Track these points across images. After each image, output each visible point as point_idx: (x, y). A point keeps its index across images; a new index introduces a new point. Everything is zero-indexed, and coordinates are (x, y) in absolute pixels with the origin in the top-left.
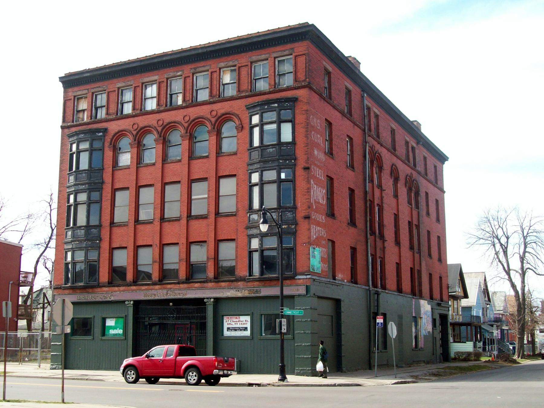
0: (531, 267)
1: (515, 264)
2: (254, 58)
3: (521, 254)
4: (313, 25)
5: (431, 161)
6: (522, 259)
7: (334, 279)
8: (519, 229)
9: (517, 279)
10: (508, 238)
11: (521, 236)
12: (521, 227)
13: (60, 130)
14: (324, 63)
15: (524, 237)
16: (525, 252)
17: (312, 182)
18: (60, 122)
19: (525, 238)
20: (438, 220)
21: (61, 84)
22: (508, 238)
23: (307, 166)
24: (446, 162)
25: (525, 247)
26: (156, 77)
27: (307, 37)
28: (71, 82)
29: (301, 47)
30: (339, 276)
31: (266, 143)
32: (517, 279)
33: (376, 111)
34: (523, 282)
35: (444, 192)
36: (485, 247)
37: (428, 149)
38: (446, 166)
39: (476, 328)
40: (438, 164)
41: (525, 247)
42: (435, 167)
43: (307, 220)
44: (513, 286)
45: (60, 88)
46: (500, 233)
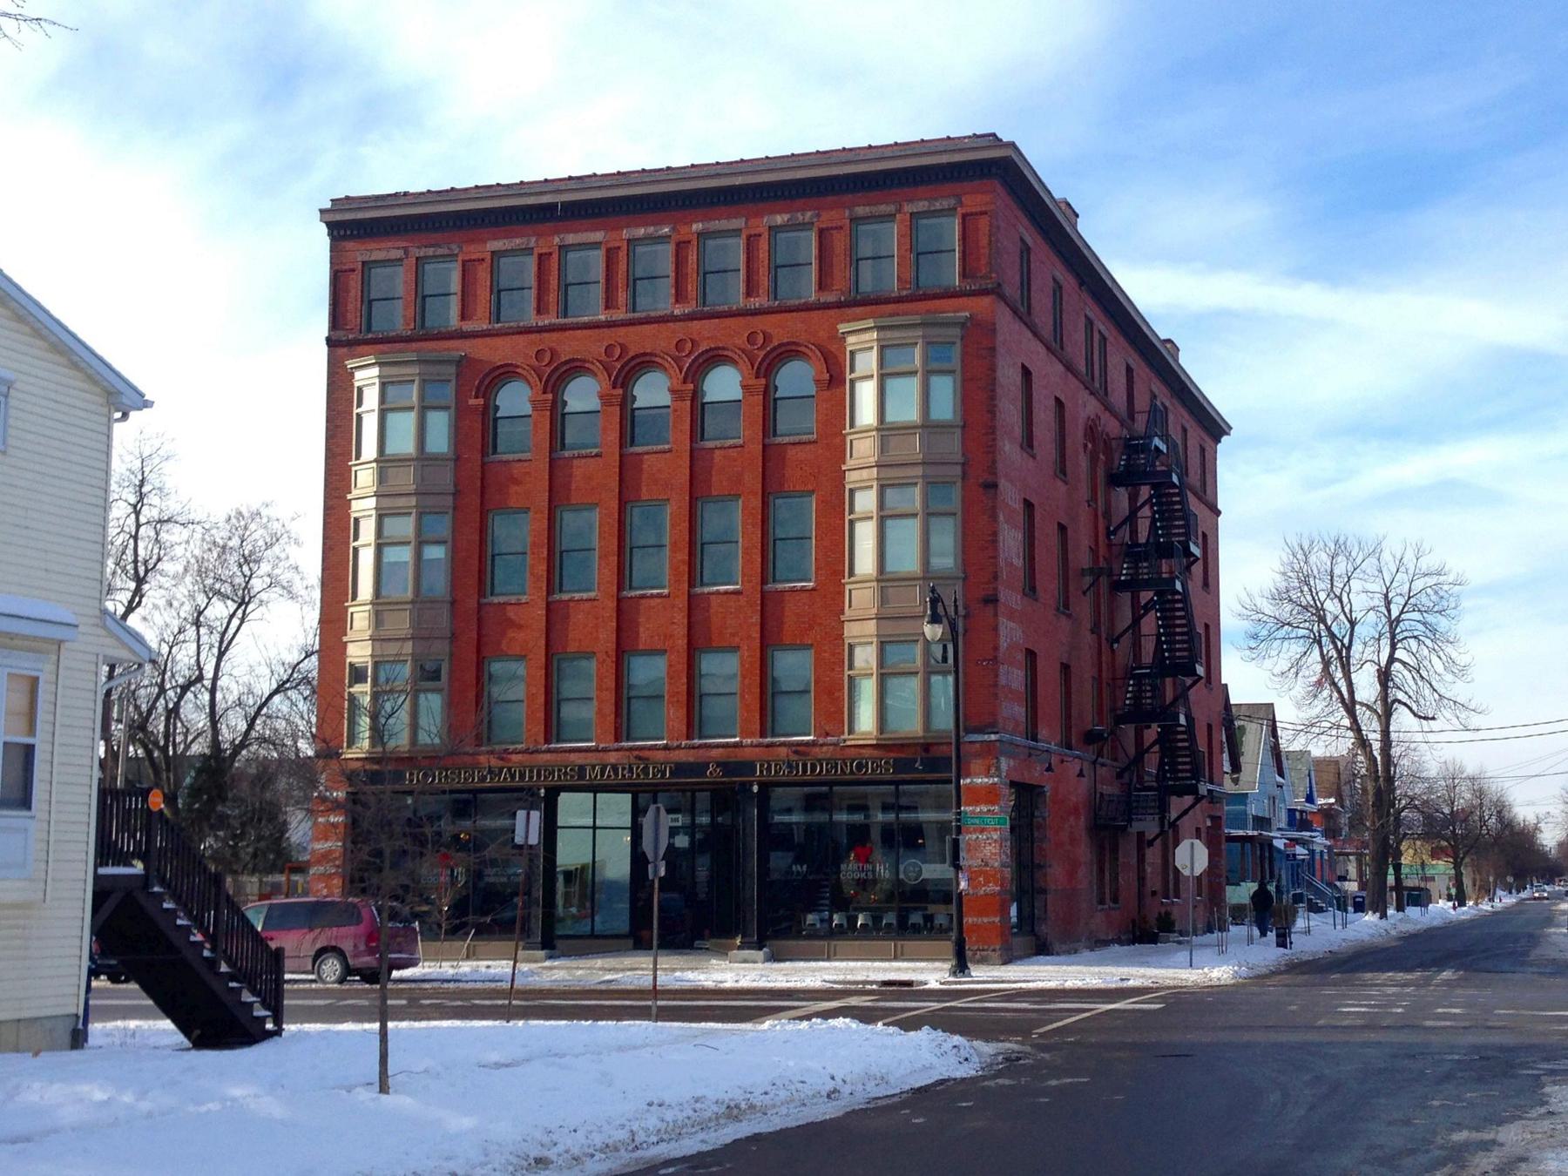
0: (1404, 698)
1: (1366, 686)
2: (861, 211)
3: (1383, 664)
4: (1012, 145)
5: (1195, 435)
6: (1385, 676)
7: (1034, 738)
8: (1378, 601)
9: (1371, 729)
10: (1353, 623)
11: (1384, 620)
12: (1386, 596)
13: (325, 348)
14: (1022, 230)
15: (1391, 623)
16: (1392, 659)
17: (1001, 518)
18: (324, 330)
19: (1393, 623)
20: (1206, 584)
21: (323, 229)
22: (1353, 623)
23: (990, 479)
24: (1224, 439)
25: (1393, 647)
26: (598, 236)
27: (994, 170)
28: (357, 227)
29: (977, 198)
30: (1043, 732)
31: (891, 417)
32: (1371, 729)
33: (1102, 328)
34: (1386, 733)
35: (1218, 513)
36: (1296, 648)
37: (1191, 412)
38: (1224, 446)
39: (1262, 846)
40: (1209, 441)
41: (1393, 647)
42: (1203, 450)
43: (991, 606)
44: (1363, 743)
45: (320, 239)
46: (1331, 607)
